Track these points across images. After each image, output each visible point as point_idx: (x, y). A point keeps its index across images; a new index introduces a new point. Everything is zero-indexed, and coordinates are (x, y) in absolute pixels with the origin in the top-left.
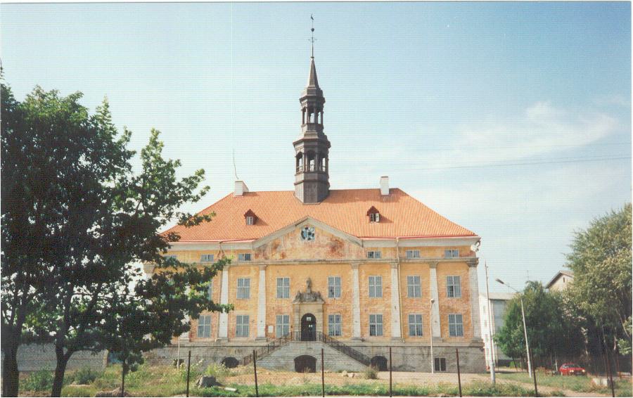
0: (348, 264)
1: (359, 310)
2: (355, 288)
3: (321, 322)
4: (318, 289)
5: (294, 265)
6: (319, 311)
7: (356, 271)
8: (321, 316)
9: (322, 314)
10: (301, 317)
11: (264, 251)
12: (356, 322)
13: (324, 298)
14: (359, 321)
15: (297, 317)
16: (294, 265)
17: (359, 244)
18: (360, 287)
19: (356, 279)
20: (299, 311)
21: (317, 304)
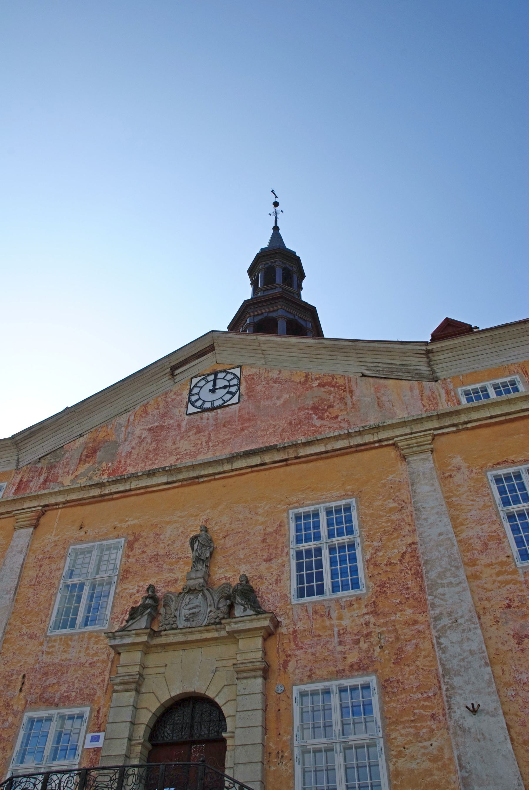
0: (380, 444)
1: (477, 637)
2: (435, 527)
3: (257, 735)
4: (244, 569)
5: (146, 490)
6: (241, 672)
7: (424, 465)
8: (257, 701)
9: (257, 684)
10: (146, 717)
11: (51, 467)
12: (474, 710)
13: (270, 601)
14: (488, 702)
15: (127, 714)
16: (146, 490)
17: (419, 377)
18: (456, 523)
19: (429, 493)
20: (137, 684)
21: (233, 636)
